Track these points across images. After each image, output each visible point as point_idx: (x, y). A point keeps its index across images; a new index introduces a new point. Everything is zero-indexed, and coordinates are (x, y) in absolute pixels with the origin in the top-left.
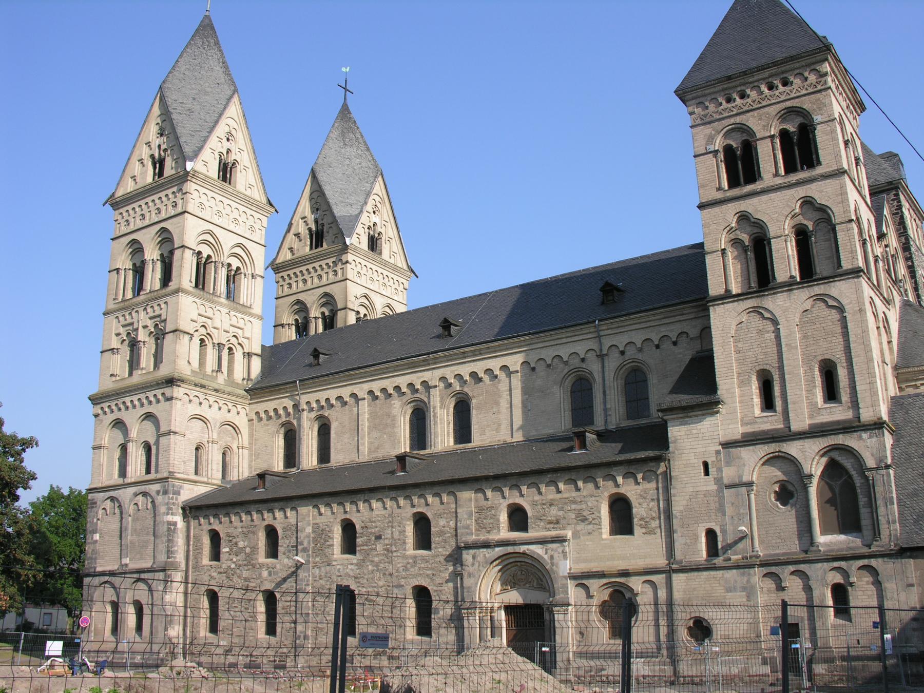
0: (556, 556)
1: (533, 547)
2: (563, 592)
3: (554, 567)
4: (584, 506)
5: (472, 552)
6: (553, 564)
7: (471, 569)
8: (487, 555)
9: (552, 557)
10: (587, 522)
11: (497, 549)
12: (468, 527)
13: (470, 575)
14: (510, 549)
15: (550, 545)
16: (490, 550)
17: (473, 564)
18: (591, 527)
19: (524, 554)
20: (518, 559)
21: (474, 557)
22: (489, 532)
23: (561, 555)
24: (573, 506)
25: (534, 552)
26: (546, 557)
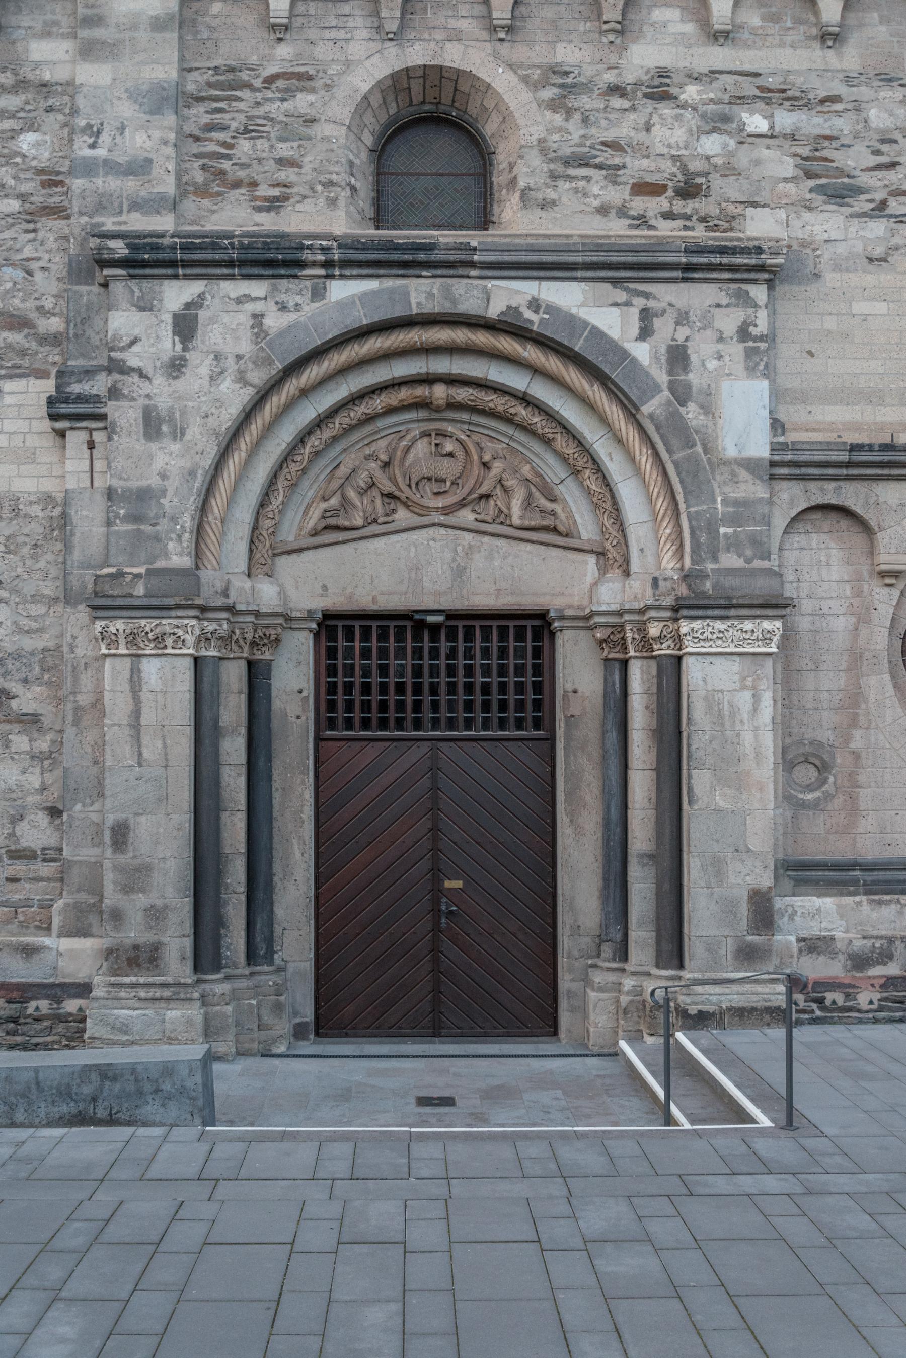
0: (702, 349)
1: (567, 296)
2: (734, 544)
3: (691, 413)
4: (842, 125)
5: (176, 294)
6: (681, 394)
7: (161, 391)
8: (274, 322)
9: (678, 357)
10: (861, 204)
11: (341, 290)
12: (140, 168)
13: (153, 424)
14: (421, 293)
15: (667, 294)
16: (294, 291)
17: (176, 367)
18: (878, 228)
19: (510, 327)
20: (442, 365)
21: (185, 326)
22: (273, 205)
23: (737, 349)
24: (786, 119)
25: (573, 323)
26: (642, 352)
